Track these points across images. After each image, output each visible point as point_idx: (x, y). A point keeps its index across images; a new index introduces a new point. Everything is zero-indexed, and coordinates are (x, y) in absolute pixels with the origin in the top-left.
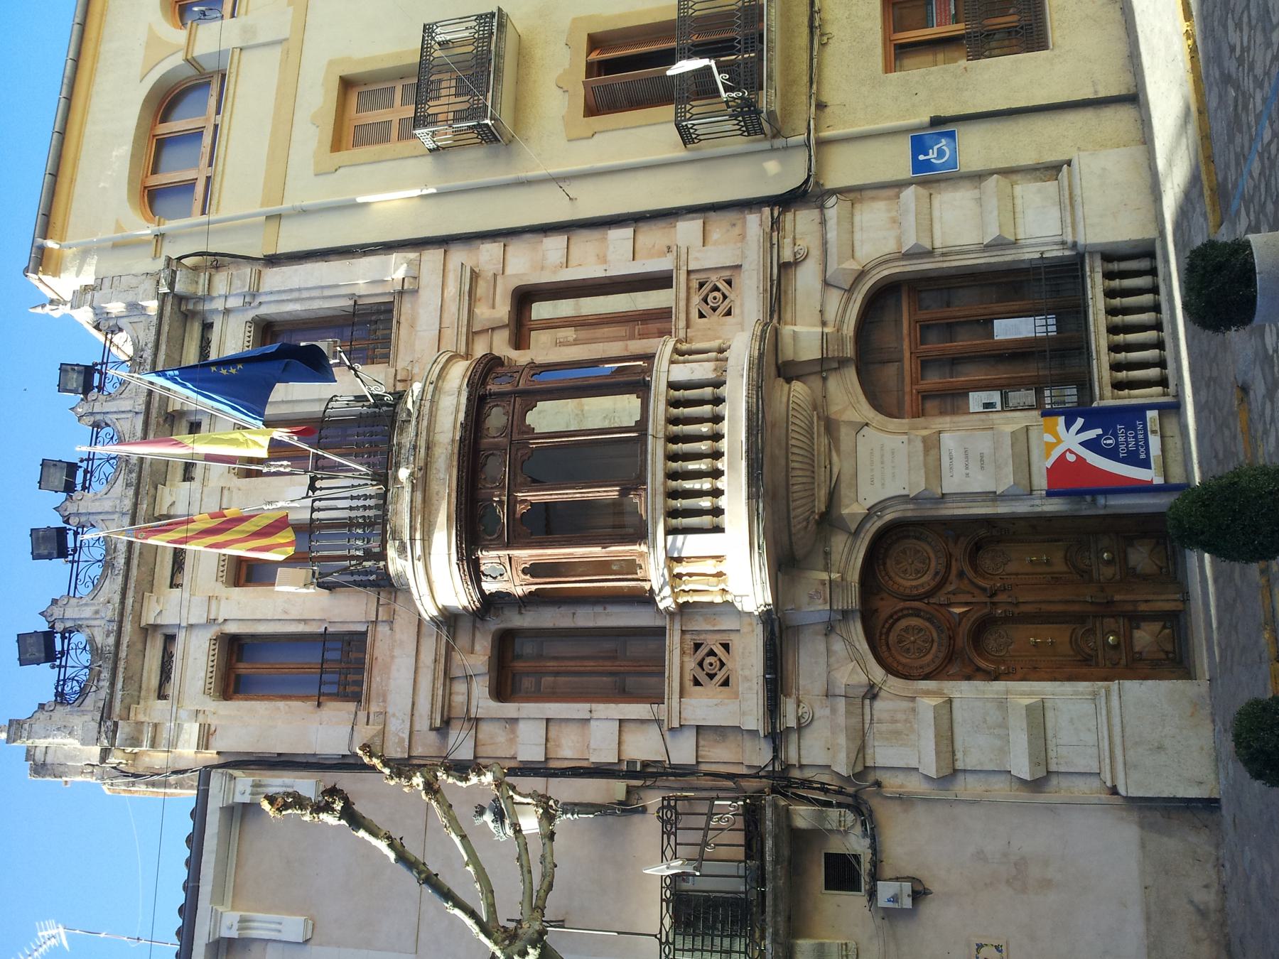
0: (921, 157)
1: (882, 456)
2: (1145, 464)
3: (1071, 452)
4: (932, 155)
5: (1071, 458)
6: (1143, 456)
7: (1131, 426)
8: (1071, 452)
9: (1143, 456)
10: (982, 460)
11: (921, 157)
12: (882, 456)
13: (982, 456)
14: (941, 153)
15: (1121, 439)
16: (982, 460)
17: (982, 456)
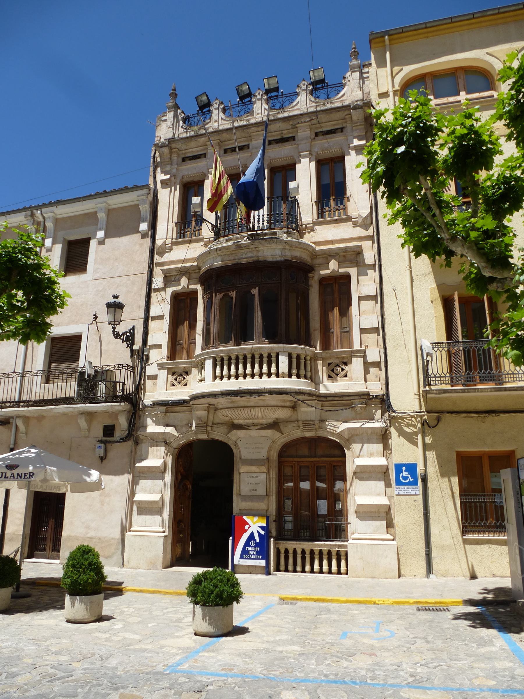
0: (404, 468)
1: (258, 448)
2: (242, 557)
3: (249, 528)
4: (405, 474)
5: (246, 527)
6: (244, 556)
7: (258, 553)
8: (249, 528)
9: (244, 556)
10: (254, 490)
11: (404, 468)
12: (258, 448)
13: (256, 490)
14: (405, 478)
15: (253, 549)
16: (254, 490)
17: (256, 490)
